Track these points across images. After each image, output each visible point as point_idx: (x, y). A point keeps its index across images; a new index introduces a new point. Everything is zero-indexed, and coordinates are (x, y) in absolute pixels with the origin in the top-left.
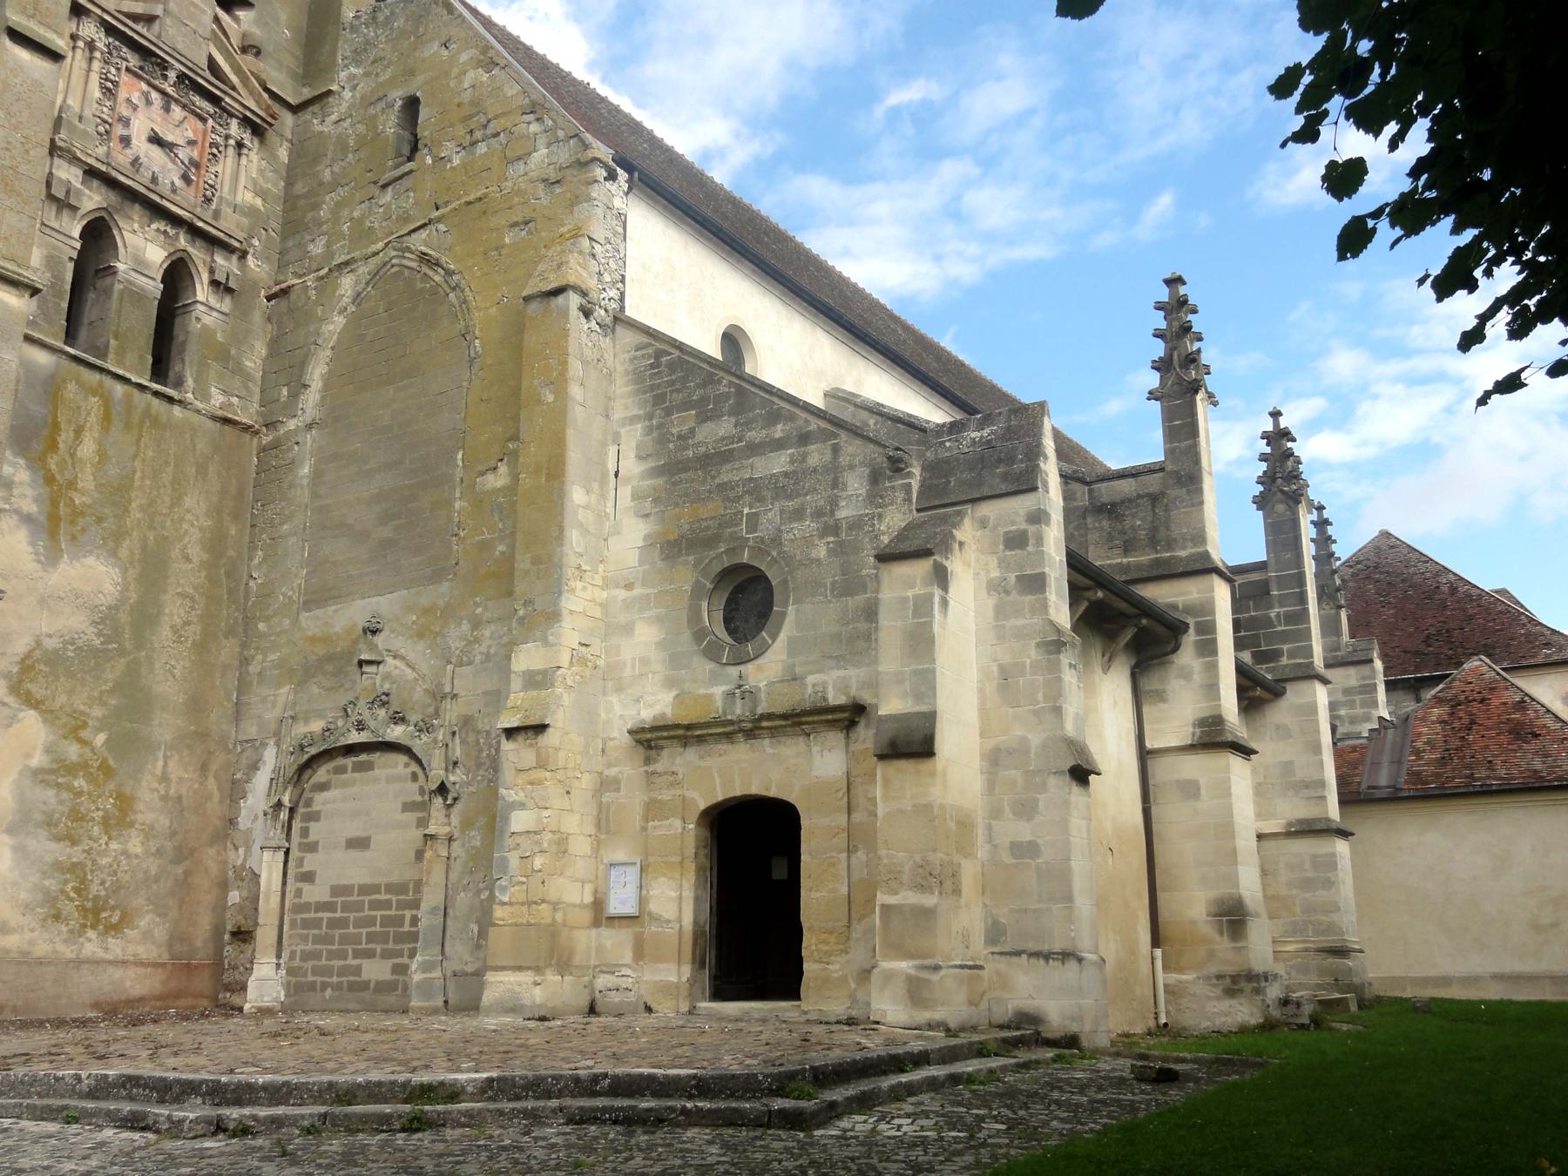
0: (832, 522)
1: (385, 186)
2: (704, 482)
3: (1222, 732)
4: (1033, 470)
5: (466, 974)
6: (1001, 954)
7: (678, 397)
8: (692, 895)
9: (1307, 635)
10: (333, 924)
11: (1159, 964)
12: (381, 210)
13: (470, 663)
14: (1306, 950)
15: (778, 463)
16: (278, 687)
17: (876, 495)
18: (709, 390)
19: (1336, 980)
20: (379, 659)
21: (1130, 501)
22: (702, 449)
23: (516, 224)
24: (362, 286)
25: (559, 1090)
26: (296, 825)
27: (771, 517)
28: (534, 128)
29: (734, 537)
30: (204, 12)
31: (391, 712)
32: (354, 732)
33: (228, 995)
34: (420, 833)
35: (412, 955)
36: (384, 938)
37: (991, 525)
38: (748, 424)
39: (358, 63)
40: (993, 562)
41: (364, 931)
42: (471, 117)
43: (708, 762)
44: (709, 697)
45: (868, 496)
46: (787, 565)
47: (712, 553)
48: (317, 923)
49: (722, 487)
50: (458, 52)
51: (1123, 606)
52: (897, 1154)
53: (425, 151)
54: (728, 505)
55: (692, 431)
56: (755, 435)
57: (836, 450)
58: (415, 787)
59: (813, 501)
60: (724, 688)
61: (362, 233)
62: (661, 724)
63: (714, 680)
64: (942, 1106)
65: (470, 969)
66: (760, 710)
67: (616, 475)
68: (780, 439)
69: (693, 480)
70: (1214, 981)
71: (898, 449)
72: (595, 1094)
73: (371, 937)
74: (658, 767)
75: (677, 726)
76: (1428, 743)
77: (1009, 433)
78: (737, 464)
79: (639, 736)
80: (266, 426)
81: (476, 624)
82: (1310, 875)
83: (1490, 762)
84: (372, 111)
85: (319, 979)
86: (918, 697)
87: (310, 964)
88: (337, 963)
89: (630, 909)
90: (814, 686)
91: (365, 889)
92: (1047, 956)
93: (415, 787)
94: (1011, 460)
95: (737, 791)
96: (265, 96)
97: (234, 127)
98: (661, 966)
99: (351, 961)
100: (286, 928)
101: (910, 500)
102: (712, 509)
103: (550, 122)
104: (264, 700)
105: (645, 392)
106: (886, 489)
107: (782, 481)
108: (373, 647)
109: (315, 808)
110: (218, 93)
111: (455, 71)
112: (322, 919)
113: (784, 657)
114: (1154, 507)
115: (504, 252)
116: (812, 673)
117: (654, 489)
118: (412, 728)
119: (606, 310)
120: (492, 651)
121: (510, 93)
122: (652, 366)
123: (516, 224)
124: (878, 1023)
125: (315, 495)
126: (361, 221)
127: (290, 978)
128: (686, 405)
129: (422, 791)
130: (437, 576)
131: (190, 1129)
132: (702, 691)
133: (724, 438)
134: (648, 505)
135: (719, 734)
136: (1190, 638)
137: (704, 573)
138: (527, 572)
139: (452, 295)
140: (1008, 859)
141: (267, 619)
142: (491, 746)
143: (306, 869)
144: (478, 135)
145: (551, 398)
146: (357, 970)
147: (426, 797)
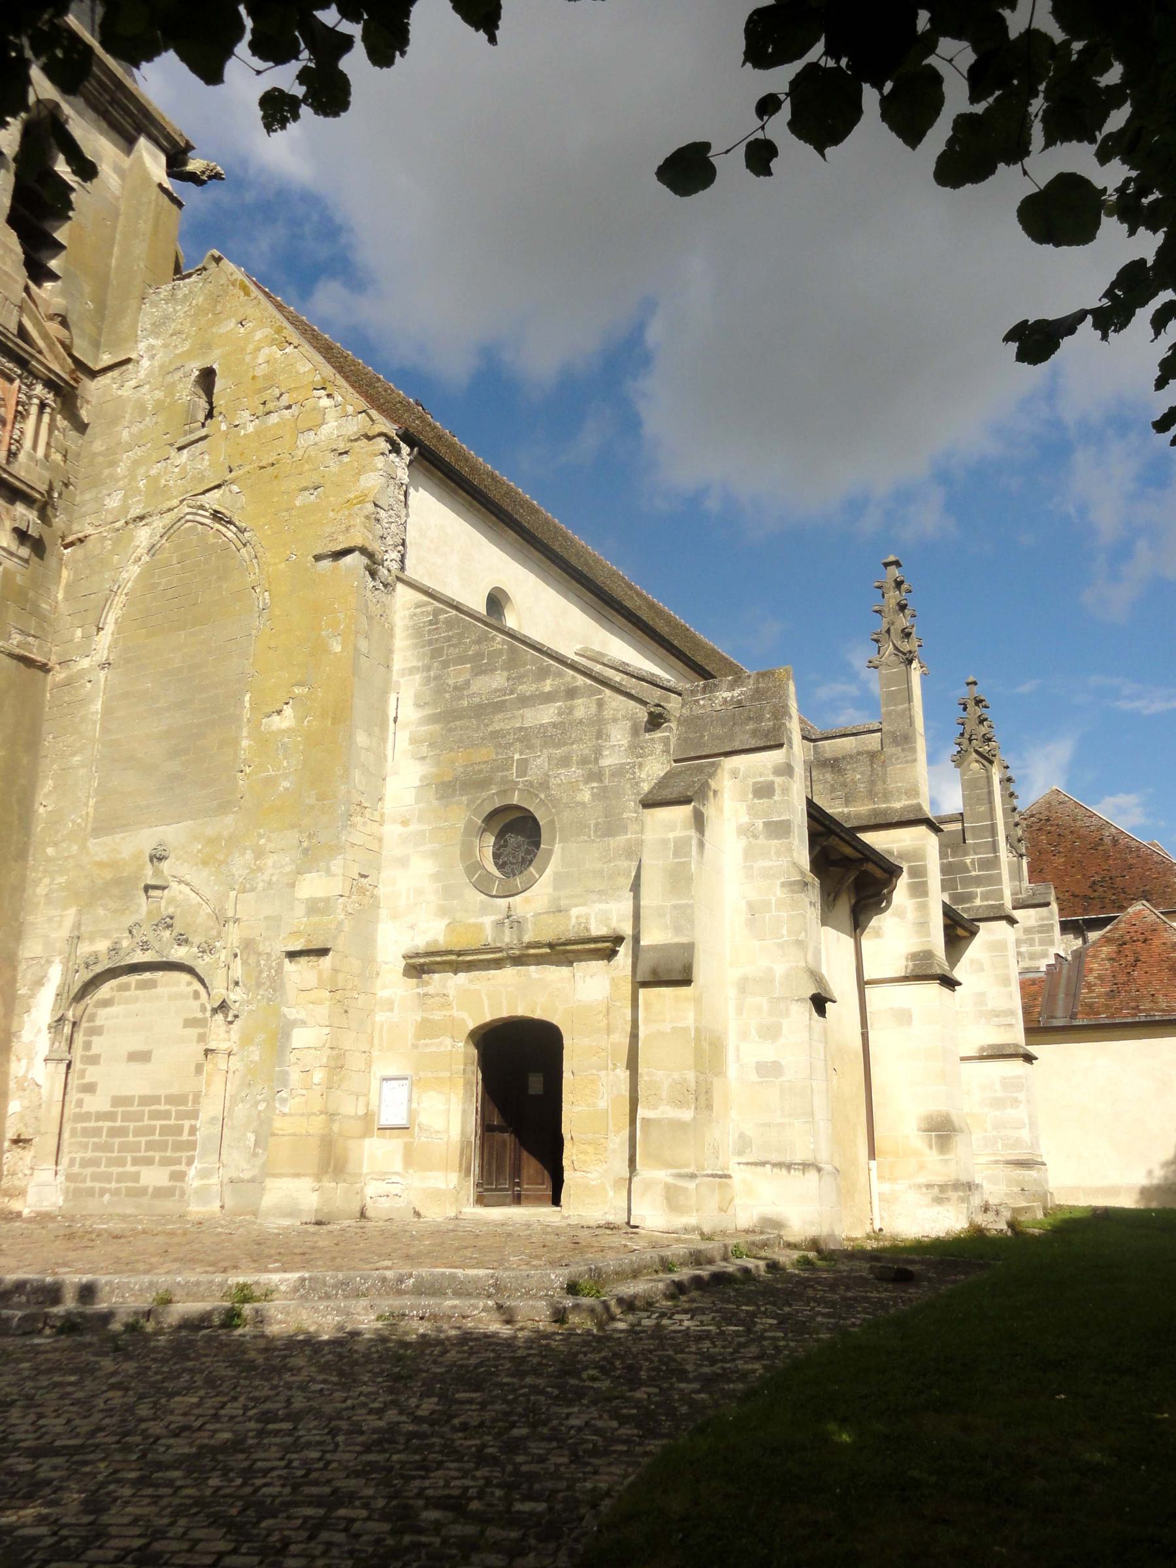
0: (596, 769)
1: (180, 449)
2: (477, 729)
3: (931, 965)
4: (780, 727)
5: (242, 1181)
6: (748, 1164)
7: (455, 652)
8: (460, 1108)
9: (998, 880)
10: (113, 1133)
11: (874, 1174)
12: (177, 470)
13: (253, 890)
14: (996, 1162)
15: (547, 715)
16: (65, 908)
17: (636, 749)
18: (484, 646)
19: (1023, 1190)
20: (166, 884)
21: (851, 756)
22: (477, 700)
23: (306, 489)
24: (158, 538)
25: (367, 1289)
26: (79, 1038)
27: (539, 763)
28: (325, 402)
29: (504, 780)
30: (15, 281)
31: (175, 934)
32: (139, 952)
33: (7, 1199)
34: (202, 1047)
35: (190, 1162)
36: (162, 1146)
37: (741, 774)
38: (520, 678)
39: (157, 335)
40: (743, 808)
41: (143, 1139)
42: (266, 389)
44: (480, 927)
45: (629, 747)
46: (554, 807)
47: (484, 795)
48: (97, 1132)
49: (495, 735)
50: (253, 331)
51: (848, 851)
52: (688, 1346)
54: (500, 751)
55: (467, 683)
56: (526, 688)
57: (600, 704)
58: (196, 1004)
59: (579, 749)
61: (157, 490)
62: (432, 950)
63: (484, 910)
64: (713, 1303)
65: (247, 1175)
66: (527, 939)
67: (395, 720)
68: (549, 693)
69: (467, 728)
70: (924, 1190)
71: (658, 705)
72: (400, 1293)
73: (150, 1146)
74: (431, 989)
75: (450, 952)
76: (1099, 977)
77: (758, 694)
78: (509, 715)
79: (413, 961)
80: (60, 664)
81: (259, 854)
82: (1000, 1094)
83: (1153, 995)
84: (169, 379)
85: (97, 1185)
86: (678, 929)
87: (88, 1171)
88: (116, 1170)
89: (402, 1122)
90: (577, 917)
91: (145, 1100)
92: (789, 1167)
93: (196, 1004)
94: (759, 718)
95: (505, 1014)
96: (69, 361)
97: (39, 389)
98: (429, 1174)
99: (130, 1168)
100: (66, 1135)
101: (668, 752)
102: (486, 753)
103: (340, 398)
104: (50, 919)
105: (423, 646)
106: (646, 741)
108: (157, 873)
109: (98, 1022)
110: (26, 356)
111: (250, 348)
112: (101, 1128)
113: (550, 890)
114: (872, 762)
115: (294, 513)
116: (576, 906)
117: (431, 734)
118: (195, 950)
119: (389, 570)
120: (274, 879)
121: (302, 370)
122: (431, 623)
123: (306, 489)
124: (637, 1227)
125: (105, 730)
126: (156, 479)
127: (69, 1184)
128: (461, 660)
129: (203, 1008)
130: (223, 808)
131: (18, 1326)
132: (472, 921)
133: (496, 691)
134: (424, 750)
135: (488, 961)
136: (903, 882)
138: (312, 807)
139: (243, 551)
140: (754, 1077)
141: (56, 844)
142: (271, 968)
143: (87, 1080)
144: (271, 406)
146: (136, 1177)
147: (208, 1014)
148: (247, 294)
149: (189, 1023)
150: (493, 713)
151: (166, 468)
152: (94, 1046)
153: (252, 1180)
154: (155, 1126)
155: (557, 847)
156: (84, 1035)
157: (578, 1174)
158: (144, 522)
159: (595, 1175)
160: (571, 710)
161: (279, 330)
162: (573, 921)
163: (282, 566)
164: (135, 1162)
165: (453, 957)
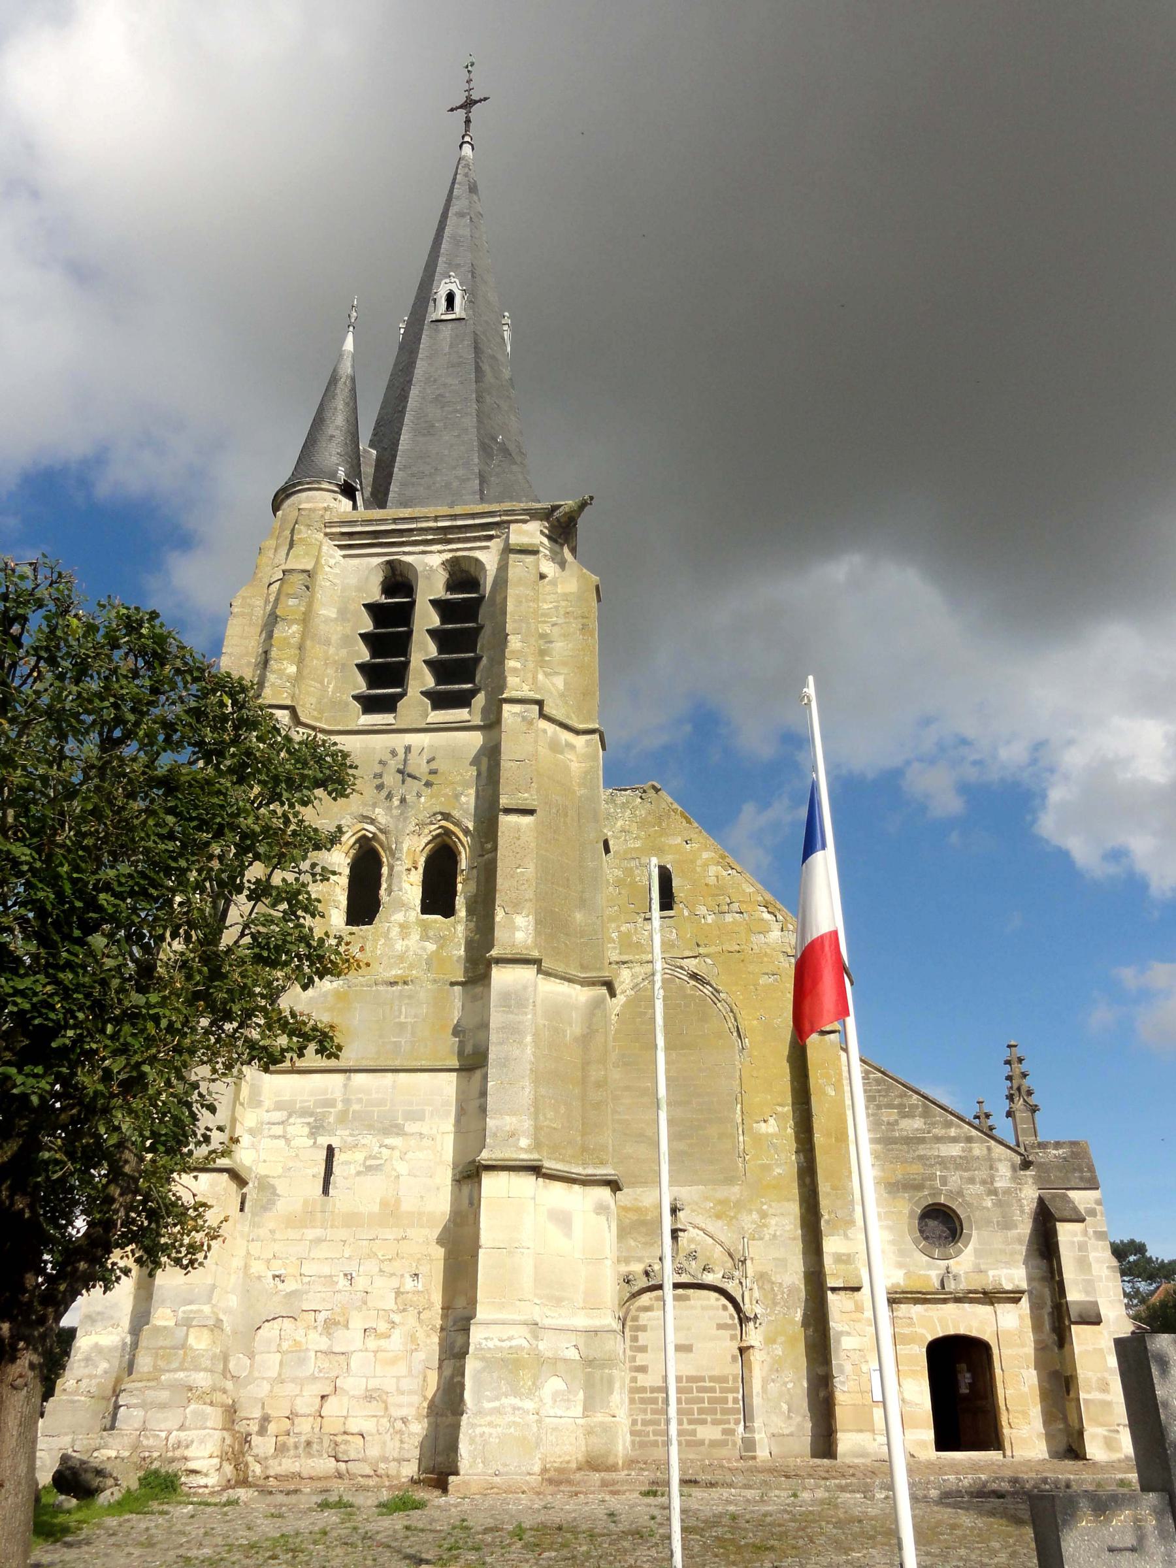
0: (992, 1188)
2: (908, 1152)
12: (646, 933)
13: (761, 1239)
15: (955, 1150)
18: (905, 1100)
23: (767, 974)
29: (932, 1187)
34: (735, 1345)
36: (713, 1411)
38: (933, 1124)
41: (695, 1407)
42: (718, 895)
43: (931, 1313)
44: (928, 1277)
47: (920, 1194)
49: (921, 1158)
53: (681, 905)
56: (938, 1131)
57: (989, 1149)
58: (726, 1314)
60: (939, 1272)
63: (929, 1267)
65: (786, 1432)
68: (954, 1137)
73: (701, 1411)
81: (764, 1215)
86: (1087, 1293)
87: (650, 1428)
95: (952, 1332)
102: (916, 1169)
107: (958, 1161)
109: (641, 1322)
111: (699, 862)
112: (657, 1398)
120: (778, 1233)
123: (767, 974)
126: (628, 934)
128: (890, 1106)
130: (730, 1181)
133: (917, 1130)
137: (917, 1204)
138: (828, 1194)
139: (719, 1005)
145: (833, 1093)
146: (694, 1433)
148: (689, 822)
149: (720, 1327)
150: (918, 1144)
151: (636, 929)
152: (640, 1338)
153: (791, 1435)
154: (704, 1398)
155: (974, 1233)
156: (630, 1331)
157: (1014, 1431)
158: (625, 966)
159: (1025, 1431)
160: (971, 1150)
161: (723, 857)
162: (991, 1279)
163: (755, 1022)
164: (690, 1422)
165: (919, 1295)
